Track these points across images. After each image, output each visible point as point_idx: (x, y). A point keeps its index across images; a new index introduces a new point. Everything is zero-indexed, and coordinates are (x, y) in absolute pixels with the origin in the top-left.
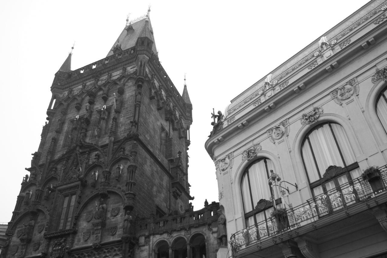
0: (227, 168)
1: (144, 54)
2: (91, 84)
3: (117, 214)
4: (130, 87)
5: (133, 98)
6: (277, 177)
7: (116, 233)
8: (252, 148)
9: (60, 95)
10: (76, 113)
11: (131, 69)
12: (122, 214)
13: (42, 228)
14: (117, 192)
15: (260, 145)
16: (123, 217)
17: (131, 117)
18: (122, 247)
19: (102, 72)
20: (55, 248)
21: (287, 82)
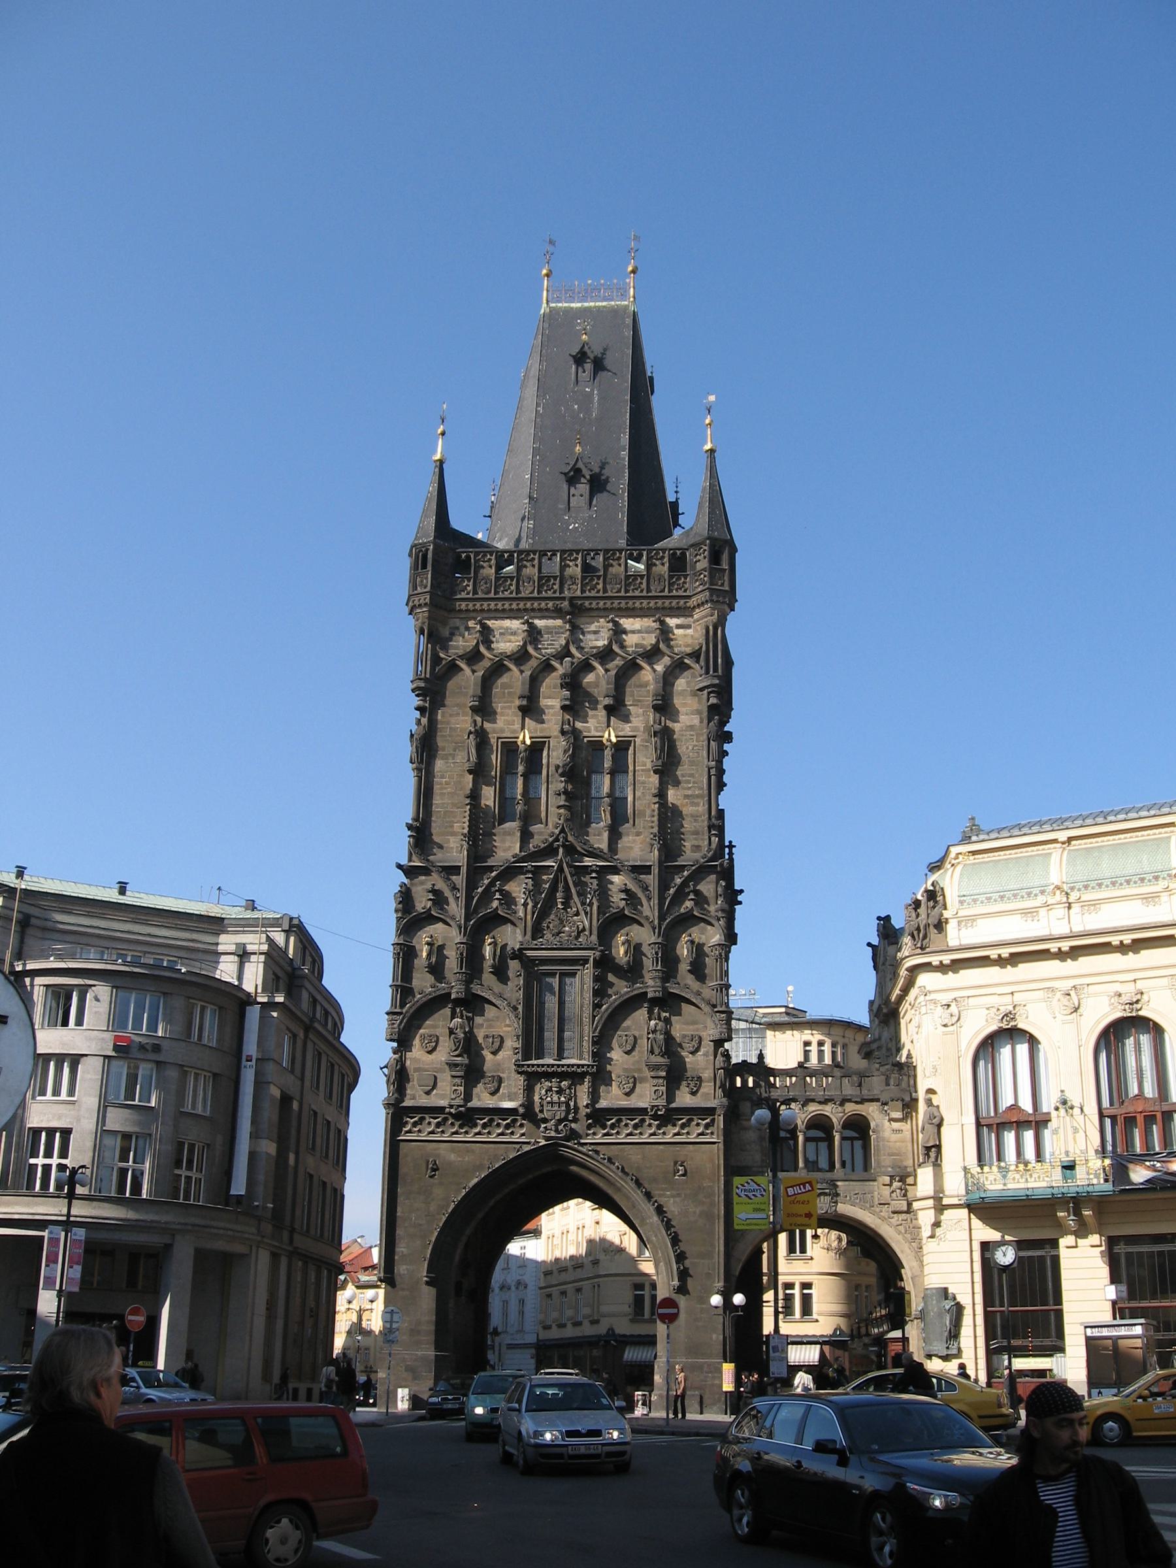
0: (953, 1025)
1: (724, 603)
2: (549, 630)
3: (697, 1050)
4: (682, 693)
5: (695, 737)
6: (1069, 1104)
7: (697, 1091)
8: (1011, 1008)
9: (440, 629)
10: (515, 718)
11: (678, 626)
12: (708, 1052)
13: (497, 1045)
14: (694, 1001)
15: (1025, 1008)
16: (712, 1058)
17: (698, 796)
18: (713, 1121)
19: (587, 603)
20: (549, 1099)
21: (1098, 906)
